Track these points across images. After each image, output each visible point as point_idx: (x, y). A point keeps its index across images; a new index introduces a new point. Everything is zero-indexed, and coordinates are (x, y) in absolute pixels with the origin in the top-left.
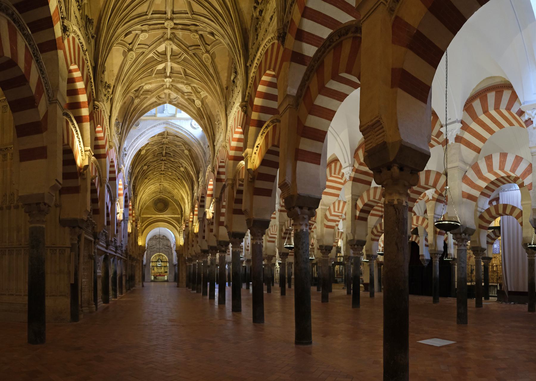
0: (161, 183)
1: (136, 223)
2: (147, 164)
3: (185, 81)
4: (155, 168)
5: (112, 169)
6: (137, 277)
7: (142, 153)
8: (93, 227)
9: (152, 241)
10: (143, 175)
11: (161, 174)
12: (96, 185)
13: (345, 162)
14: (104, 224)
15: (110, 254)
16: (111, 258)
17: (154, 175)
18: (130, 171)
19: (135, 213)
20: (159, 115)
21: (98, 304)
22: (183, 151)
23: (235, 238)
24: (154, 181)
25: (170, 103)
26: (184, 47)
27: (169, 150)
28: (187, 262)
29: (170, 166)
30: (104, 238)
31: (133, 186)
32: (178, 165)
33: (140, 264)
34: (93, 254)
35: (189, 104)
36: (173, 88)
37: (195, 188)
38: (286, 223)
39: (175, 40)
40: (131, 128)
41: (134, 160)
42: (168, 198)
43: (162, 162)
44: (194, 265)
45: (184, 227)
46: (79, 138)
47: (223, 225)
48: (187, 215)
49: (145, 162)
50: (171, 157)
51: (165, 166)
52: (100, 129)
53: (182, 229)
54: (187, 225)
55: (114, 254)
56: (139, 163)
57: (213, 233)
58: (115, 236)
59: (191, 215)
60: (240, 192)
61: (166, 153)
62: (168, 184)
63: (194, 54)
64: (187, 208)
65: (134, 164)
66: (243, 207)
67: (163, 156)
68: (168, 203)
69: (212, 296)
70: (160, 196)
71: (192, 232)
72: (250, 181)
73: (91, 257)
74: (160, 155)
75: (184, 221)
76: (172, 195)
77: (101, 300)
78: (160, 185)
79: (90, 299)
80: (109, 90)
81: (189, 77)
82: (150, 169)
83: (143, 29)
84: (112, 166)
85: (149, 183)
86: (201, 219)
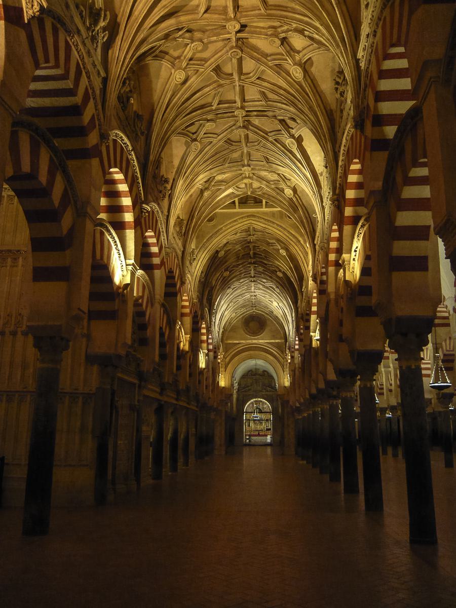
4: (241, 274)
17: (242, 283)
24: (241, 291)
26: (262, 133)
36: (254, 176)
39: (250, 127)
63: (275, 140)
67: (251, 258)
70: (253, 312)
81: (272, 164)
83: (209, 118)
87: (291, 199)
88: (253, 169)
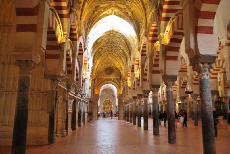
1: (94, 81)
3: (123, 3)
5: (80, 48)
7: (98, 41)
8: (67, 82)
11: (109, 54)
13: (221, 35)
15: (77, 99)
16: (78, 101)
18: (92, 51)
21: (68, 131)
22: (121, 40)
23: (154, 88)
25: (115, 14)
28: (124, 105)
30: (74, 88)
34: (66, 98)
35: (125, 14)
38: (183, 78)
44: (128, 106)
45: (122, 83)
47: (146, 81)
49: (100, 47)
51: (111, 49)
54: (124, 82)
55: (80, 99)
57: (140, 86)
60: (157, 60)
61: (112, 42)
65: (94, 47)
66: (159, 69)
69: (139, 125)
72: (164, 52)
73: (64, 100)
77: (70, 128)
79: (63, 127)
80: (80, 4)
82: (102, 51)
84: (81, 47)
87: (130, 17)
88: (116, 3)
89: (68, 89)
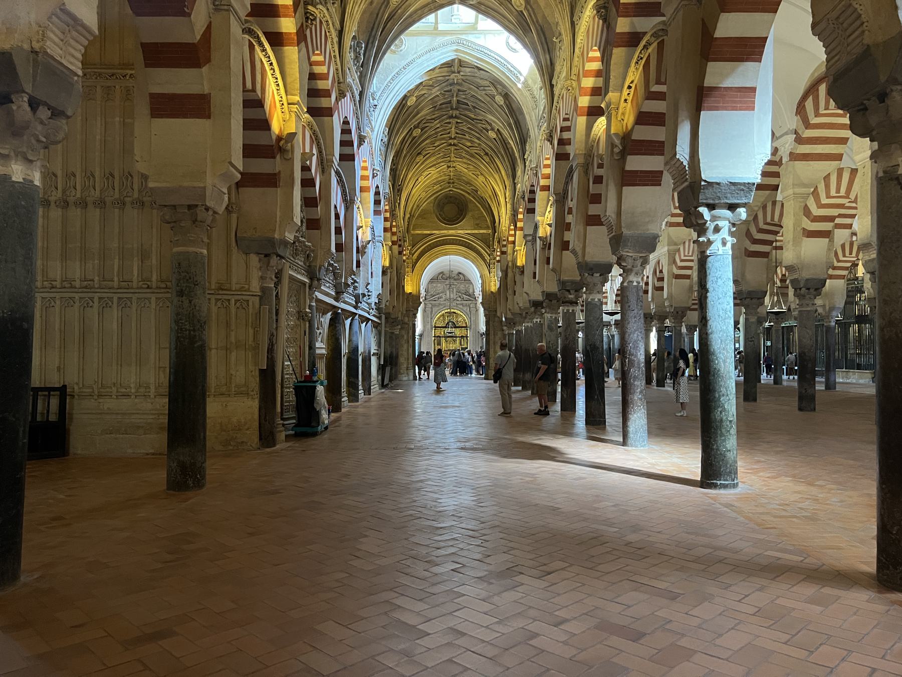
0: (451, 164)
1: (400, 246)
2: (421, 125)
4: (436, 133)
5: (346, 137)
6: (402, 360)
9: (435, 285)
10: (412, 147)
11: (451, 145)
12: (313, 171)
14: (330, 249)
15: (343, 310)
16: (347, 319)
18: (386, 140)
19: (396, 226)
20: (441, 27)
22: (493, 97)
24: (435, 160)
27: (464, 96)
29: (468, 128)
31: (391, 169)
32: (484, 126)
33: (408, 333)
37: (519, 173)
40: (384, 53)
41: (392, 117)
42: (467, 195)
43: (451, 120)
46: (277, 78)
48: (504, 228)
49: (415, 122)
50: (469, 110)
52: (320, 58)
53: (495, 258)
54: (504, 249)
56: (402, 124)
58: (354, 275)
59: (512, 230)
62: (465, 166)
64: (504, 216)
65: (393, 125)
67: (452, 109)
68: (467, 206)
71: (513, 264)
74: (447, 107)
75: (499, 242)
76: (474, 188)
78: (449, 167)
85: (426, 163)
86: (530, 238)
89: (311, 279)
